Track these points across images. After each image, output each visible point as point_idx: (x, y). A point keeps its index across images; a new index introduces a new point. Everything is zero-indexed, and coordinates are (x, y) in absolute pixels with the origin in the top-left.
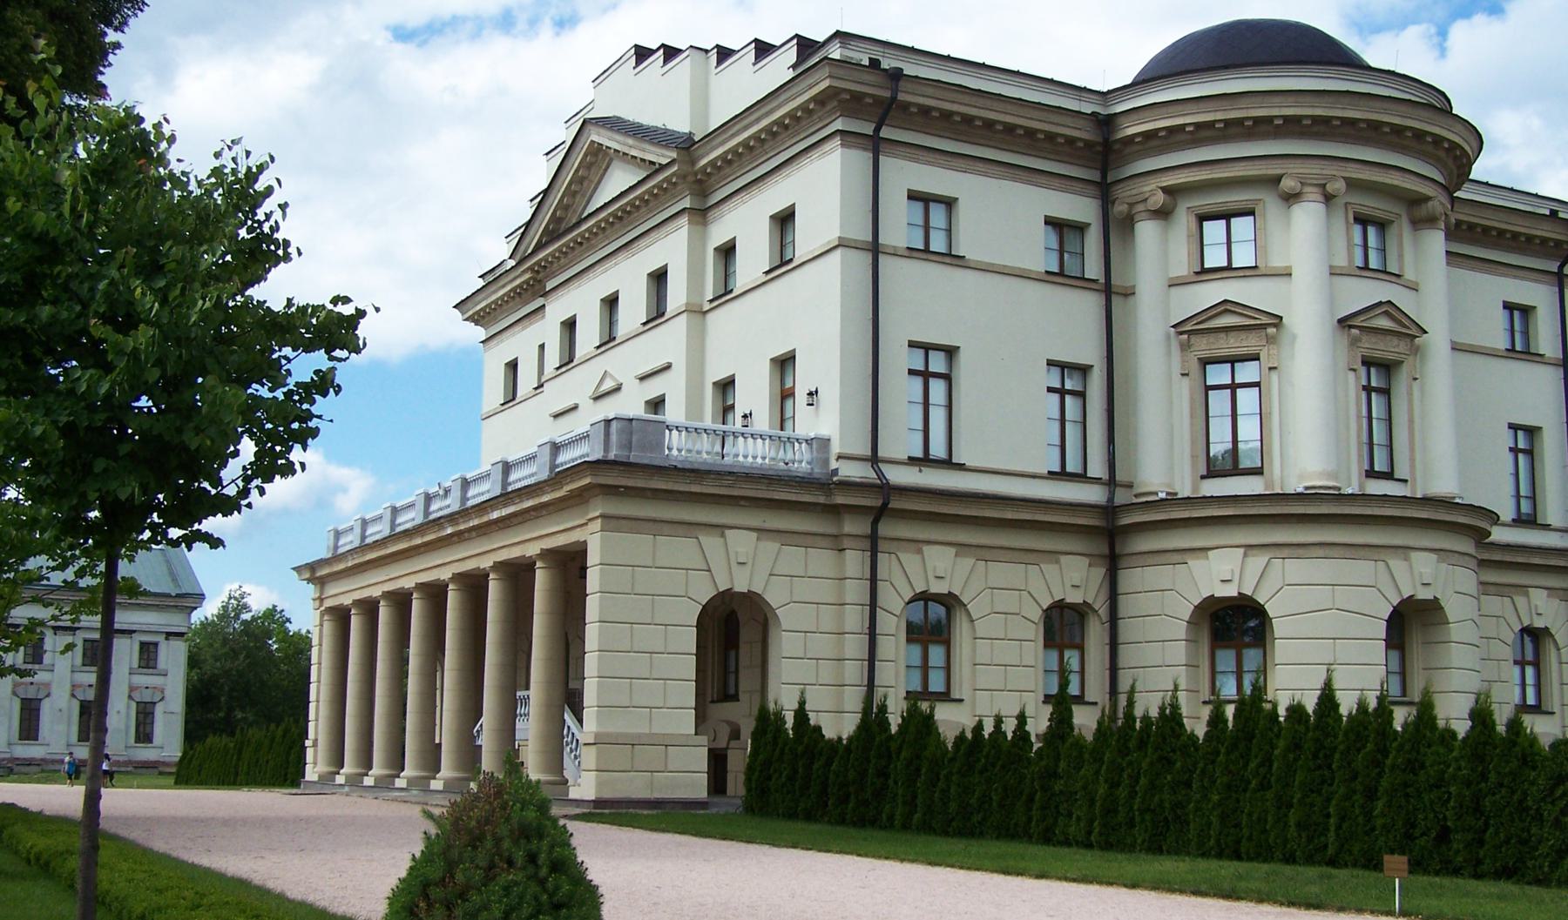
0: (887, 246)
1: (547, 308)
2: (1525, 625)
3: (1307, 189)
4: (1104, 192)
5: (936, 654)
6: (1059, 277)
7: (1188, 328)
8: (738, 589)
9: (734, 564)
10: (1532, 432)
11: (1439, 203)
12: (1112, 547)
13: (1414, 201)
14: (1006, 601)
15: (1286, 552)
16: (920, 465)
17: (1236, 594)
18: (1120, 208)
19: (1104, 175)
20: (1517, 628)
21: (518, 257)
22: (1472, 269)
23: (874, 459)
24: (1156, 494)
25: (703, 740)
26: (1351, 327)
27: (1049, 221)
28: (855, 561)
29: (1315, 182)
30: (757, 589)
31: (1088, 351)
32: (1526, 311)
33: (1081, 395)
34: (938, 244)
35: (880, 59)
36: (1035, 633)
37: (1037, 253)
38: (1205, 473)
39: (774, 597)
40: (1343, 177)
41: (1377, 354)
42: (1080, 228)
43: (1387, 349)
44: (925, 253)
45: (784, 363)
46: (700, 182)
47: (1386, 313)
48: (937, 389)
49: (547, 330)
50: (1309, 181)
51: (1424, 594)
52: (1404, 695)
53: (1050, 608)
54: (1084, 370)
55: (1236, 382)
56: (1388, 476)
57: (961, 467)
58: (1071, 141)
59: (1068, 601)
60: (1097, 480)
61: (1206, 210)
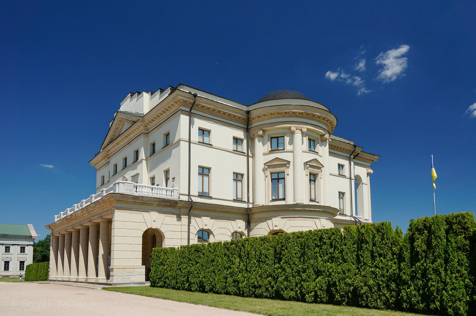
6: (236, 151)
12: (249, 217)
23: (189, 195)
25: (144, 266)
37: (231, 146)
38: (271, 200)
39: (163, 229)
42: (242, 140)
43: (315, 171)
44: (203, 143)
53: (233, 233)
54: (242, 175)
55: (279, 178)
57: (211, 198)
58: (239, 118)
59: (238, 231)
60: (245, 202)
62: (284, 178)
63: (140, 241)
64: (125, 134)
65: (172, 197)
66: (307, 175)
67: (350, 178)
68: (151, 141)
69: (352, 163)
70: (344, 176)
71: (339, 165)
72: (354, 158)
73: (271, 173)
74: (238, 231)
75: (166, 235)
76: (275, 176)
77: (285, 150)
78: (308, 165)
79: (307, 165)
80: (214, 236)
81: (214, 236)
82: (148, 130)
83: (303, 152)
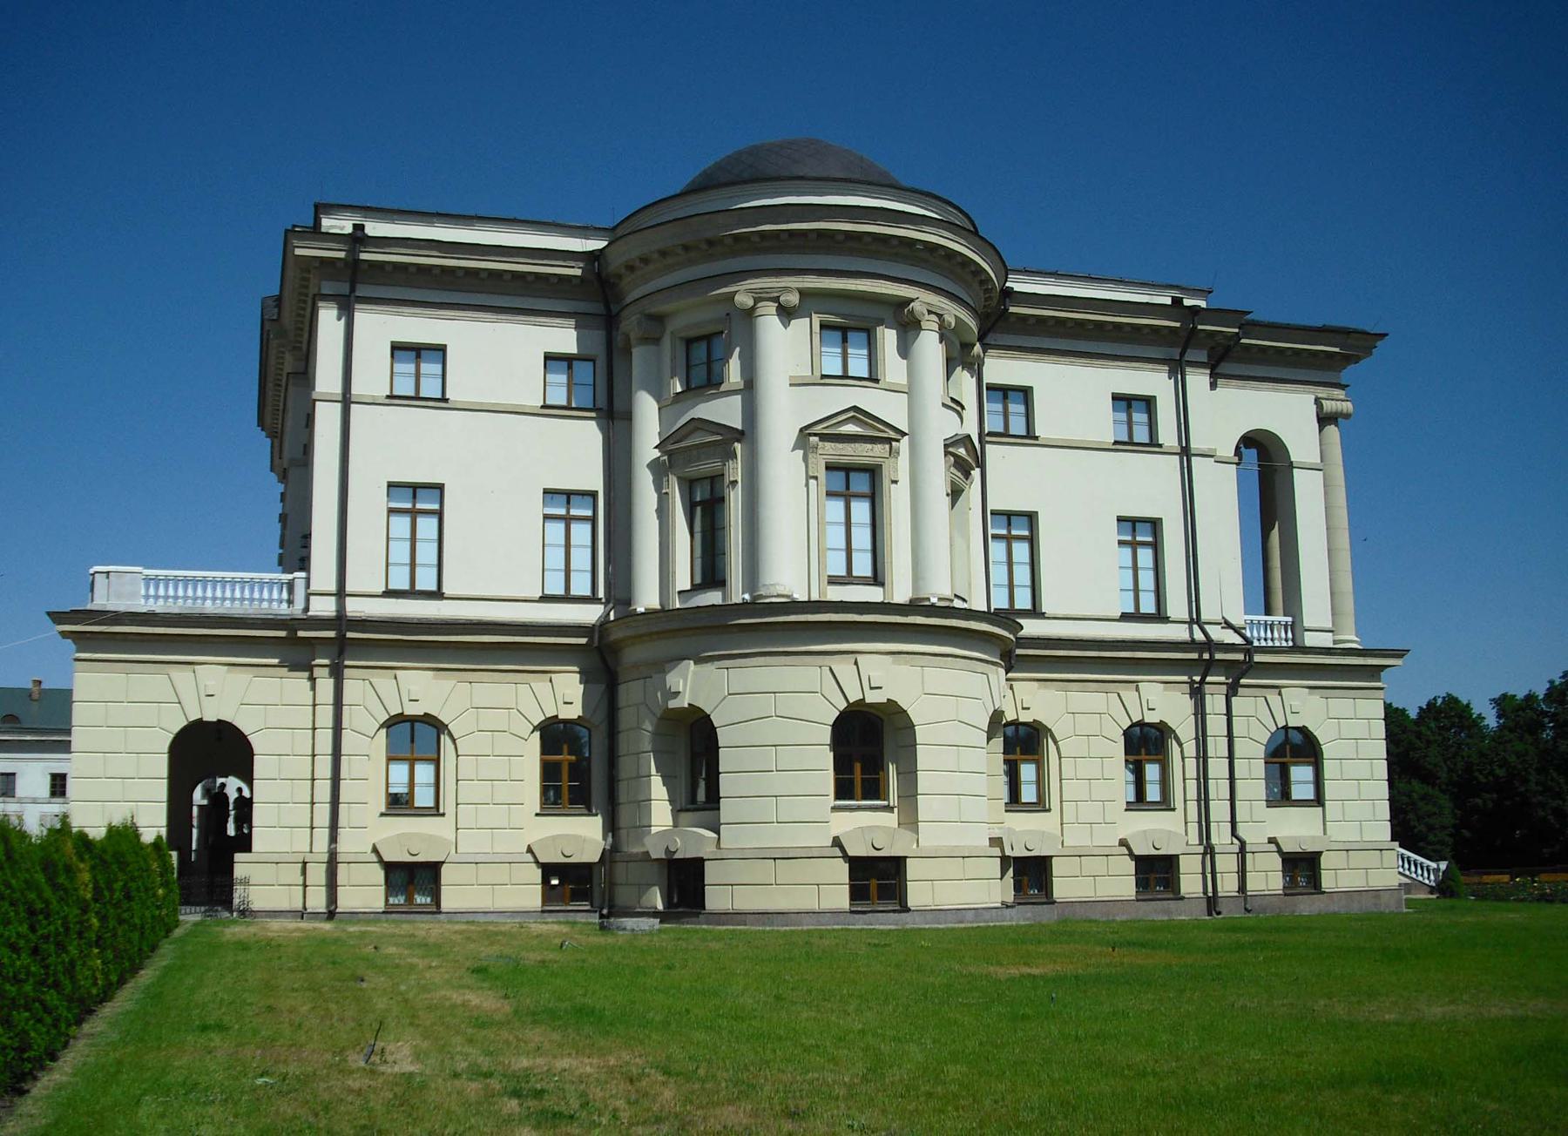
5: (424, 772)
8: (204, 719)
10: (1155, 525)
14: (491, 719)
18: (619, 340)
23: (341, 594)
26: (810, 435)
28: (326, 685)
30: (227, 716)
31: (592, 477)
32: (1149, 403)
33: (593, 520)
40: (797, 289)
48: (427, 526)
59: (560, 717)
66: (816, 478)
74: (560, 717)
78: (815, 435)
79: (811, 438)
80: (454, 741)
81: (454, 741)
83: (791, 385)
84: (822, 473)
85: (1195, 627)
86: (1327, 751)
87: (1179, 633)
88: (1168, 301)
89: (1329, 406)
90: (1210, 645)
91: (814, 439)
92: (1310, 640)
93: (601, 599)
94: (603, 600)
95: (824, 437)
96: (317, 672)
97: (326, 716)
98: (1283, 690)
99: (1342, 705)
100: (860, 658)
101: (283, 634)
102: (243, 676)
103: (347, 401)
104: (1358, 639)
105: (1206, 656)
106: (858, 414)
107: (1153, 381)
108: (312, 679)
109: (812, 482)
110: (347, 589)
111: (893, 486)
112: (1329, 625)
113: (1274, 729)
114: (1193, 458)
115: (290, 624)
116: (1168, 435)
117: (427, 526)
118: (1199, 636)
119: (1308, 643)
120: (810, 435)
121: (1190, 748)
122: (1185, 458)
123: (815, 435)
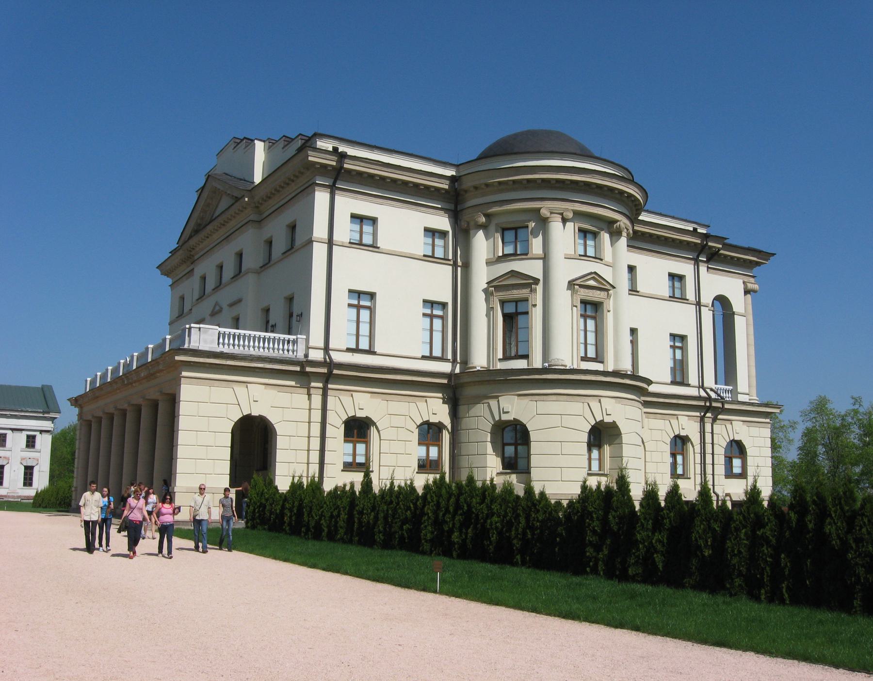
0: (337, 241)
1: (195, 270)
2: (676, 434)
3: (553, 215)
4: (455, 216)
5: (361, 448)
6: (430, 258)
7: (495, 284)
8: (253, 414)
9: (252, 401)
10: (683, 338)
11: (623, 222)
12: (454, 393)
13: (611, 222)
15: (537, 398)
16: (352, 352)
17: (512, 419)
18: (464, 225)
19: (456, 207)
20: (672, 436)
21: (180, 243)
22: (653, 256)
23: (326, 349)
24: (476, 368)
27: (427, 230)
28: (317, 399)
29: (558, 212)
32: (681, 278)
34: (368, 239)
35: (339, 147)
36: (415, 436)
37: (420, 245)
38: (502, 357)
39: (273, 418)
41: (589, 298)
42: (443, 234)
44: (359, 244)
45: (290, 300)
46: (257, 207)
47: (593, 278)
49: (194, 282)
50: (554, 211)
51: (608, 419)
52: (600, 470)
53: (422, 424)
54: (444, 305)
56: (596, 359)
58: (438, 189)
59: (430, 421)
61: (505, 226)
62: (527, 313)
63: (227, 440)
64: (220, 220)
65: (293, 354)
66: (576, 306)
67: (698, 304)
68: (266, 236)
69: (703, 269)
70: (683, 299)
71: (672, 276)
72: (708, 261)
73: (503, 303)
74: (430, 421)
75: (279, 429)
76: (510, 309)
77: (529, 256)
78: (577, 285)
80: (379, 431)
81: (379, 431)
82: (261, 214)
83: (565, 258)
84: (579, 304)
85: (701, 389)
86: (749, 451)
87: (693, 392)
88: (691, 229)
89: (750, 286)
90: (709, 398)
91: (576, 287)
92: (741, 398)
93: (449, 360)
94: (451, 361)
95: (581, 286)
96: (312, 391)
97: (317, 416)
98: (733, 422)
99: (755, 430)
100: (602, 399)
101: (298, 369)
102: (272, 392)
103: (330, 243)
104: (758, 399)
105: (708, 404)
106: (595, 276)
107: (685, 268)
108: (309, 395)
109: (575, 308)
110: (330, 347)
111: (608, 313)
112: (747, 392)
113: (728, 441)
114: (702, 307)
115: (302, 364)
116: (691, 295)
117: (365, 315)
118: (703, 394)
119: (739, 400)
120: (574, 284)
121: (698, 448)
122: (698, 307)
123: (577, 285)
